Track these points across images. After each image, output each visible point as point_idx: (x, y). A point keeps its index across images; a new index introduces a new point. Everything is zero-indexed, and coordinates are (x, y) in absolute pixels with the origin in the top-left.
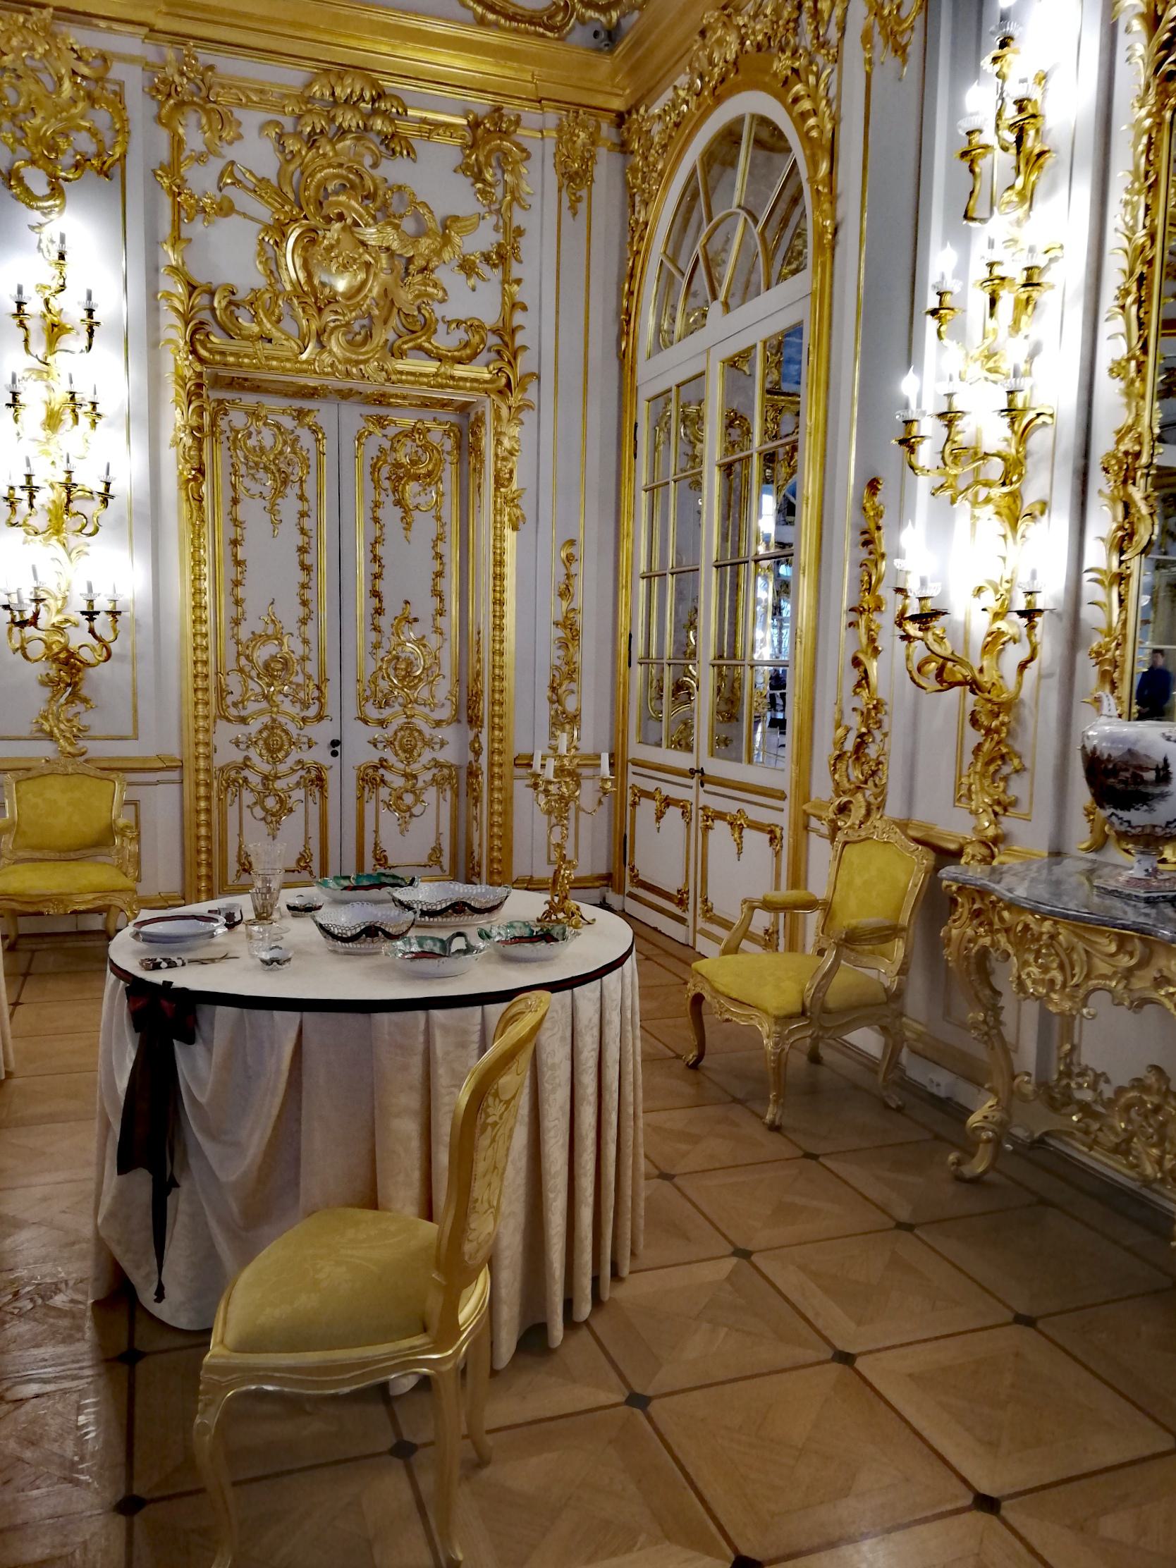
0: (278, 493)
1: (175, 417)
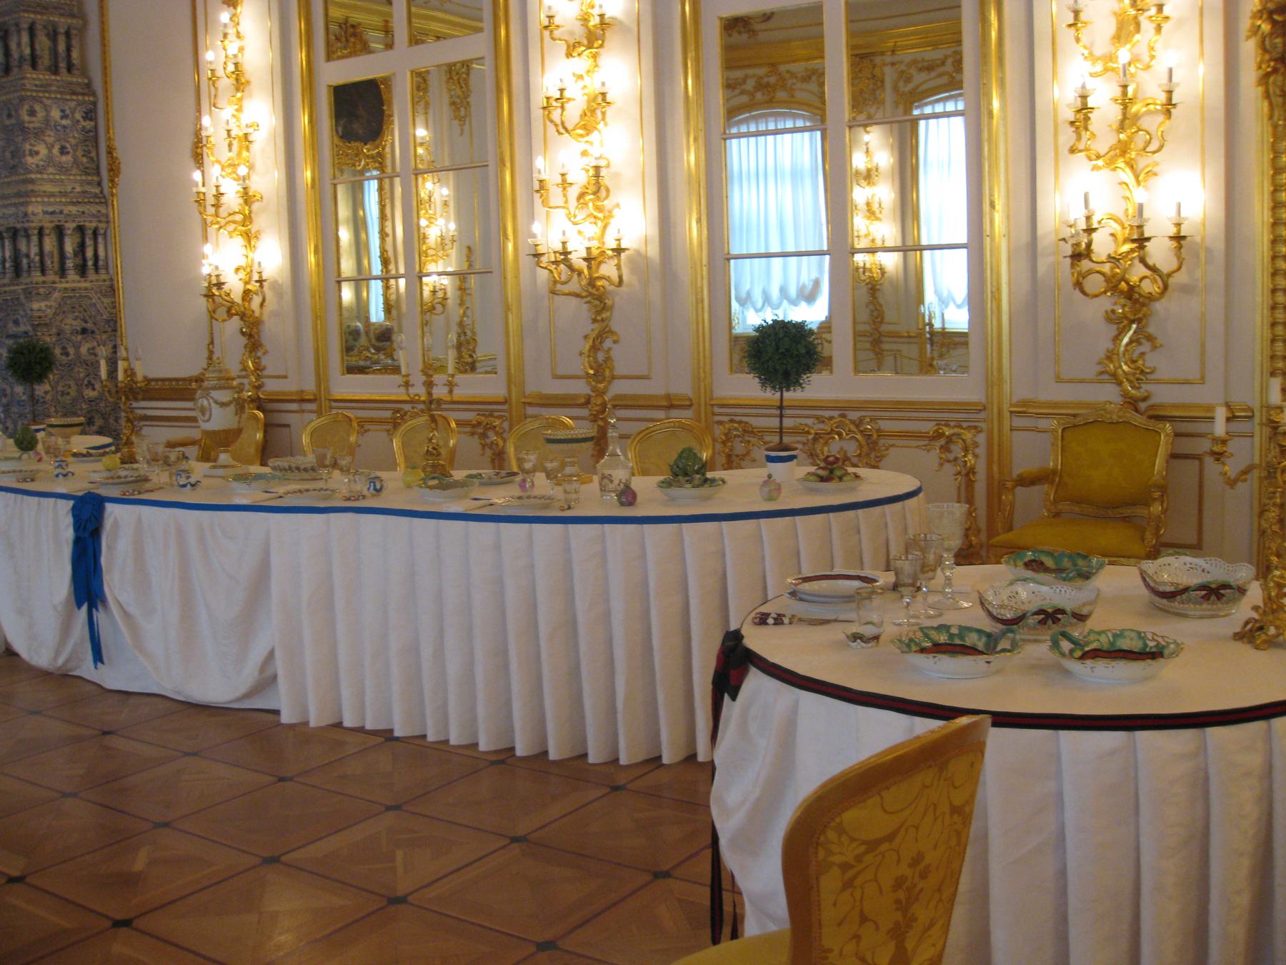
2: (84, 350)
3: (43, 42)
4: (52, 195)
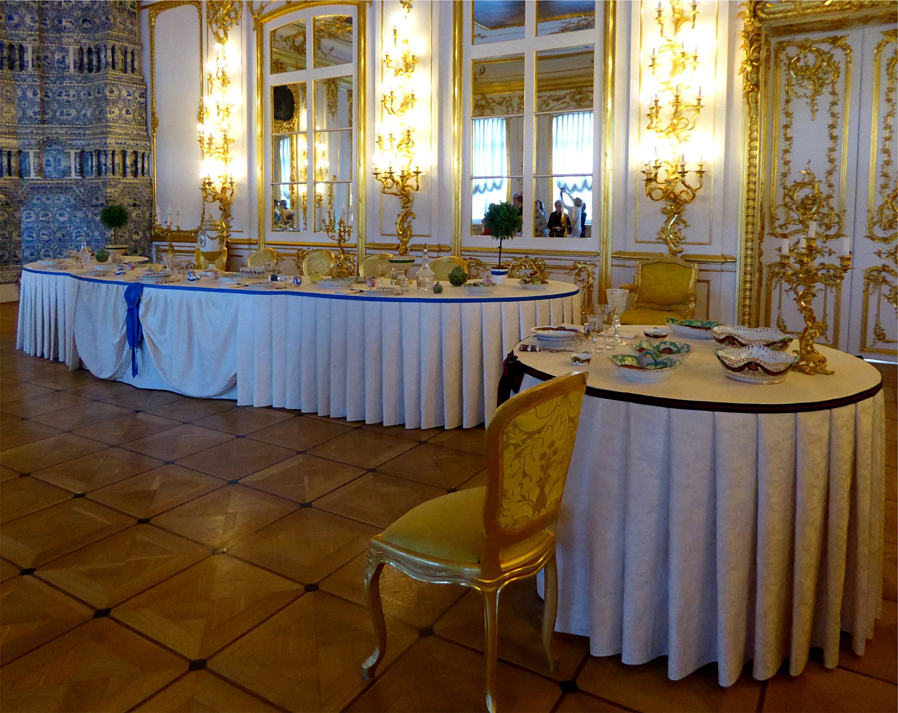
0: (817, 92)
1: (742, 55)
3: (119, 56)
4: (121, 134)
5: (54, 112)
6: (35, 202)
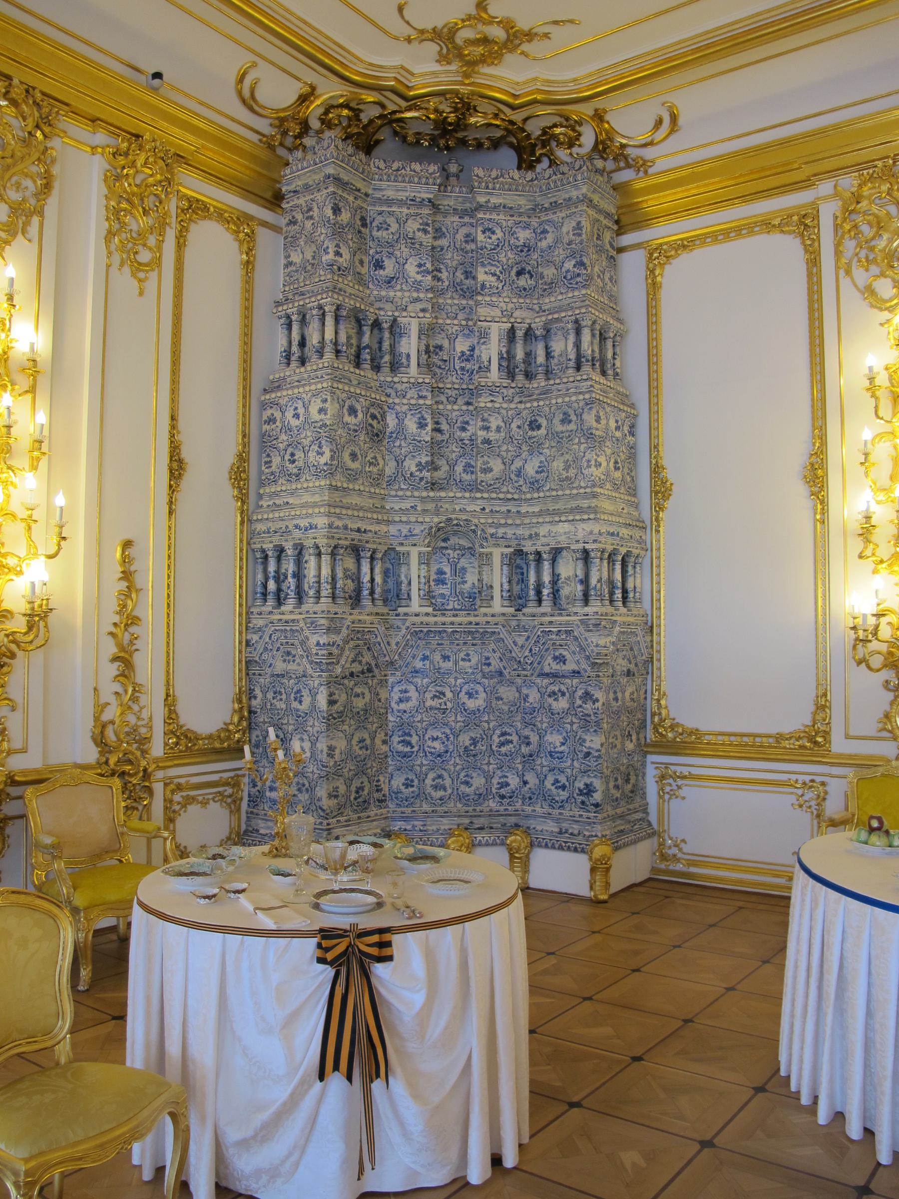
2: (627, 694)
5: (452, 466)
6: (419, 664)
